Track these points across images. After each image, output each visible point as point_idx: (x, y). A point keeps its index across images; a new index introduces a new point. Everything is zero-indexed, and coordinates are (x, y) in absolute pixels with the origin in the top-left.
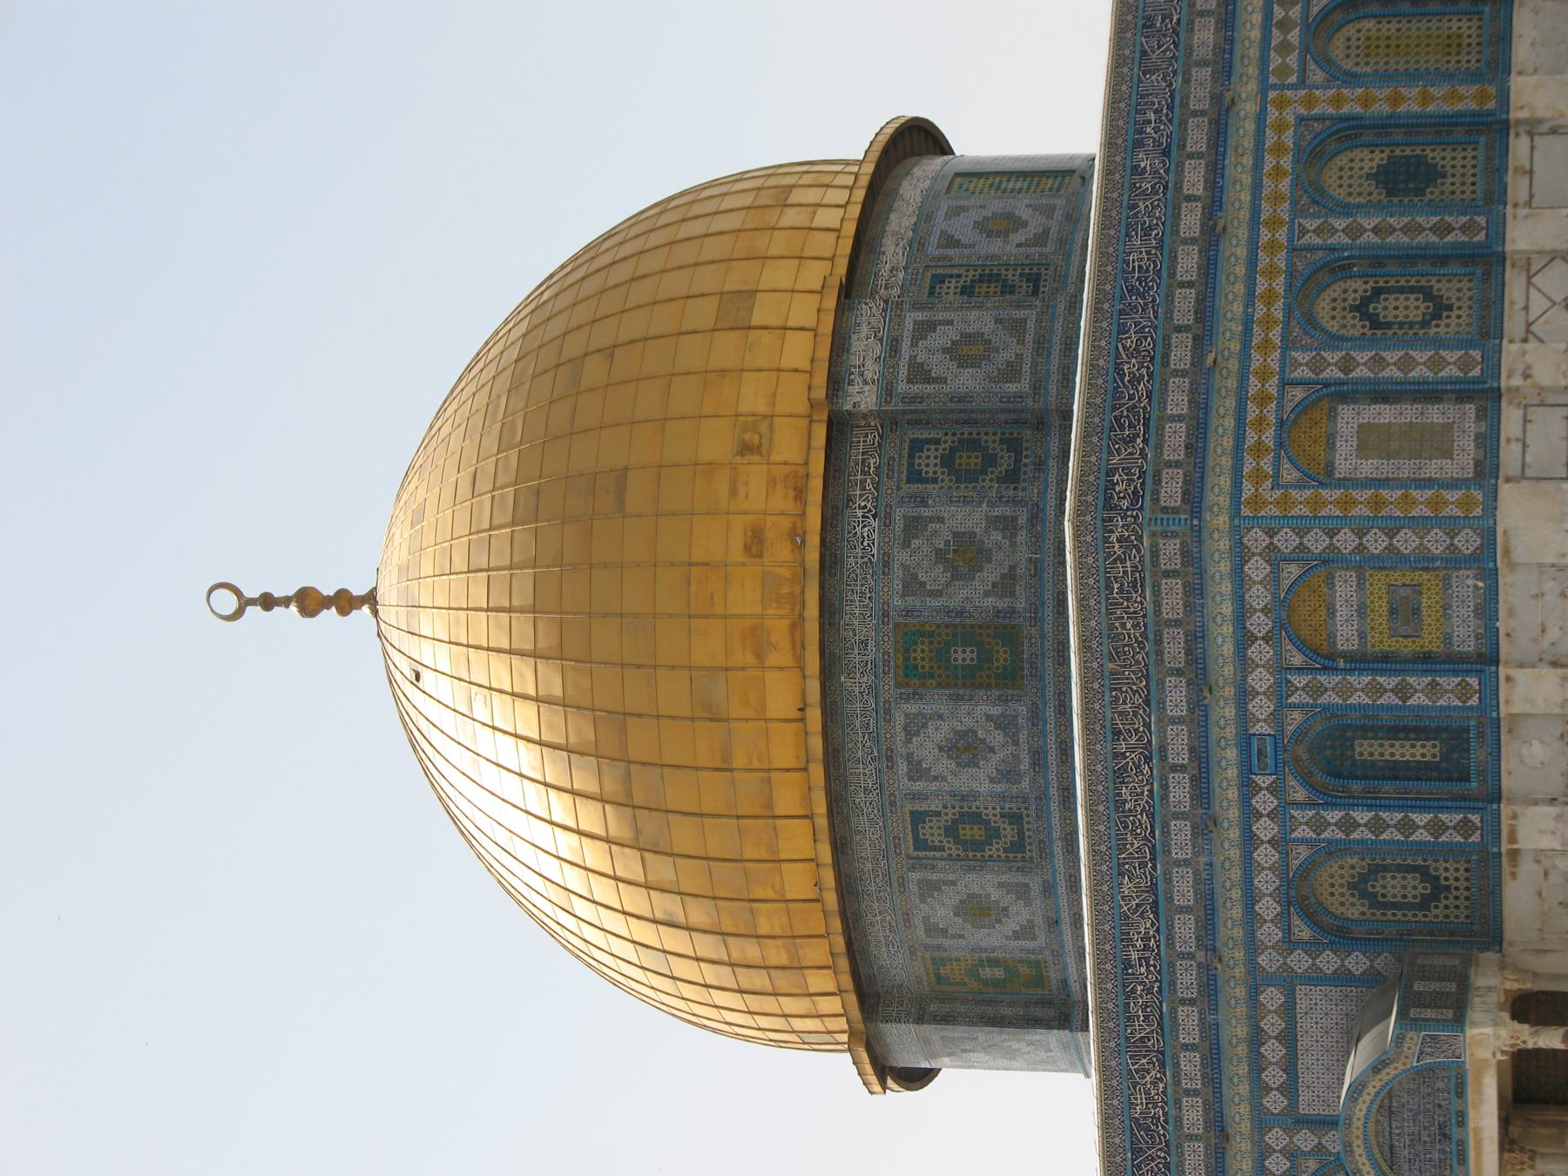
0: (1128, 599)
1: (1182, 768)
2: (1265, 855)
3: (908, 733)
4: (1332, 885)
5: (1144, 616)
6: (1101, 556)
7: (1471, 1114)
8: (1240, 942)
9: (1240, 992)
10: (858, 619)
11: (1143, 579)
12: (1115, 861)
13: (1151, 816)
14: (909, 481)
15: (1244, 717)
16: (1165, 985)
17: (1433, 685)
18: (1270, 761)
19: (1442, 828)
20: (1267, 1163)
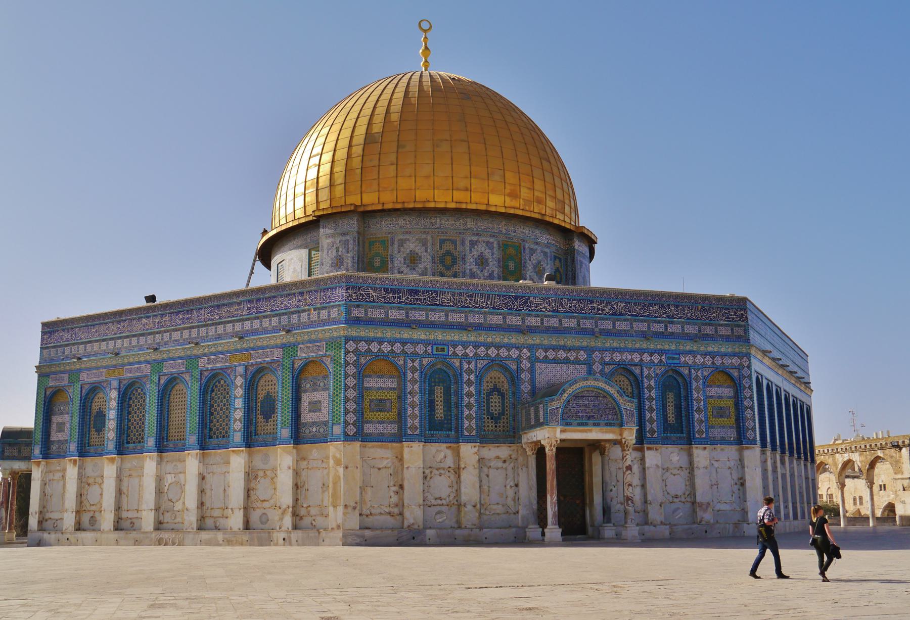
0: (723, 315)
1: (666, 329)
2: (636, 357)
3: (487, 242)
4: (620, 381)
7: (598, 428)
9: (585, 344)
10: (522, 231)
11: (730, 321)
12: (631, 301)
13: (648, 316)
14: (554, 255)
15: (686, 353)
16: (584, 315)
18: (671, 361)
19: (651, 423)
20: (514, 349)
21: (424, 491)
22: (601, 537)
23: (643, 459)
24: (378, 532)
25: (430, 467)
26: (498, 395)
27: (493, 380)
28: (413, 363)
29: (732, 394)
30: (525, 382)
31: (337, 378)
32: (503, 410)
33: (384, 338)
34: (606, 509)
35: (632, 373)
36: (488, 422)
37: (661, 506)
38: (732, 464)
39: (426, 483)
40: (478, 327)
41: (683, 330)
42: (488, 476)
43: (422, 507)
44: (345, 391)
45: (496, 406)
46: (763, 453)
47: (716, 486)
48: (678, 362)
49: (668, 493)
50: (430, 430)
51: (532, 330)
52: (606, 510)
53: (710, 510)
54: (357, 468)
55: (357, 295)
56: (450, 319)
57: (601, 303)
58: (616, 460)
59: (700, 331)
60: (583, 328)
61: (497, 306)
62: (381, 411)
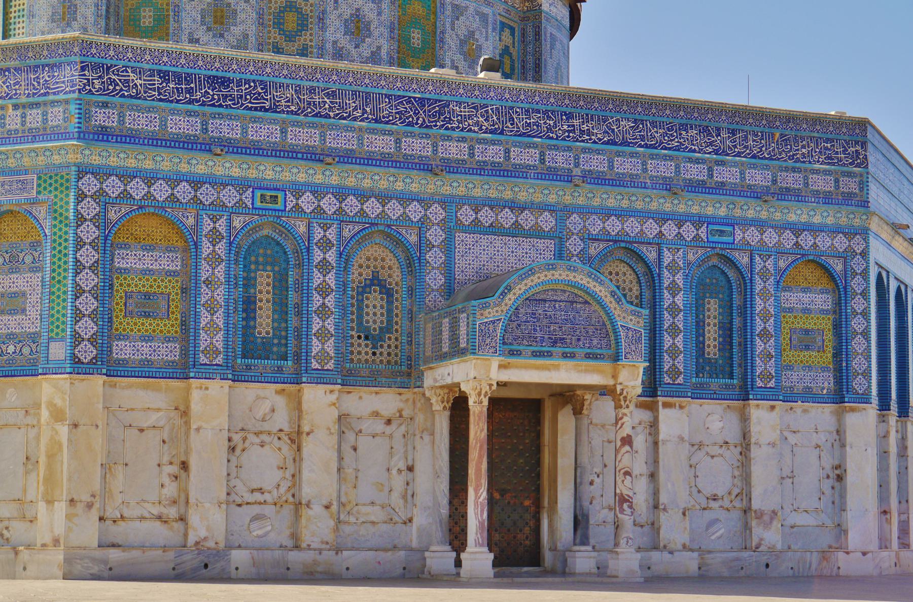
0: (820, 152)
2: (651, 229)
4: (617, 274)
5: (810, 162)
6: (847, 138)
7: (571, 363)
8: (589, 202)
9: (552, 199)
11: (833, 164)
12: (645, 118)
13: (677, 149)
15: (746, 223)
17: (770, 356)
18: (716, 238)
19: (674, 356)
20: (415, 203)
21: (228, 475)
22: (567, 570)
23: (654, 425)
24: (136, 553)
25: (243, 429)
26: (381, 293)
27: (372, 263)
28: (215, 223)
29: (829, 306)
30: (433, 268)
31: (58, 248)
32: (389, 322)
33: (156, 171)
34: (580, 518)
35: (641, 258)
36: (359, 345)
37: (684, 514)
38: (822, 438)
39: (233, 459)
40: (346, 158)
41: (743, 179)
42: (355, 449)
43: (224, 506)
44: (77, 273)
45: (375, 314)
46: (882, 419)
47: (791, 480)
48: (730, 239)
49: (699, 492)
50: (244, 356)
51: (451, 167)
52: (580, 522)
53: (776, 524)
54: (97, 426)
55: (103, 83)
56: (290, 139)
57: (587, 119)
58: (603, 426)
59: (774, 181)
60: (550, 167)
61: (384, 117)
62: (147, 315)
